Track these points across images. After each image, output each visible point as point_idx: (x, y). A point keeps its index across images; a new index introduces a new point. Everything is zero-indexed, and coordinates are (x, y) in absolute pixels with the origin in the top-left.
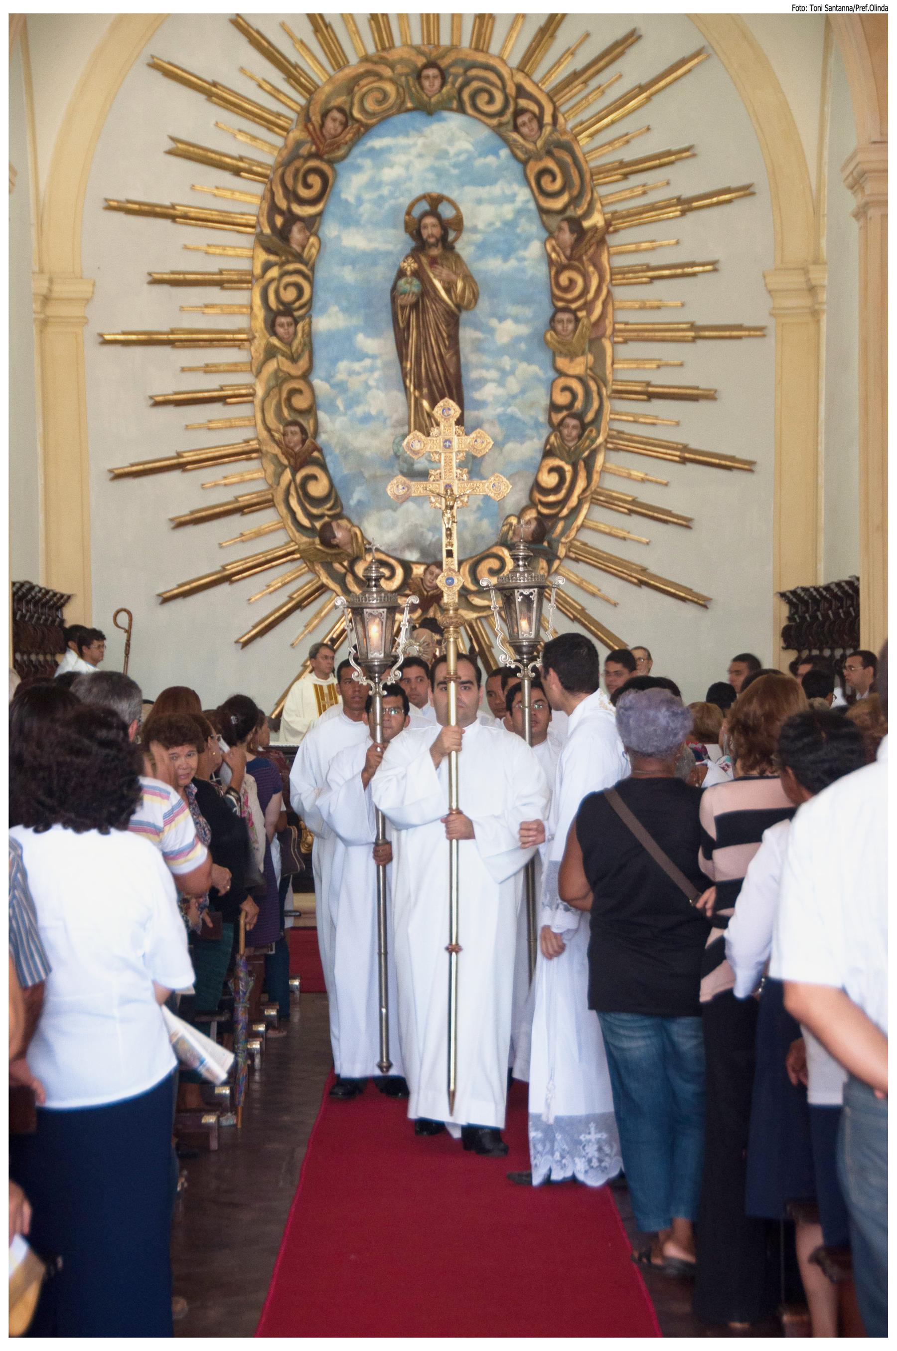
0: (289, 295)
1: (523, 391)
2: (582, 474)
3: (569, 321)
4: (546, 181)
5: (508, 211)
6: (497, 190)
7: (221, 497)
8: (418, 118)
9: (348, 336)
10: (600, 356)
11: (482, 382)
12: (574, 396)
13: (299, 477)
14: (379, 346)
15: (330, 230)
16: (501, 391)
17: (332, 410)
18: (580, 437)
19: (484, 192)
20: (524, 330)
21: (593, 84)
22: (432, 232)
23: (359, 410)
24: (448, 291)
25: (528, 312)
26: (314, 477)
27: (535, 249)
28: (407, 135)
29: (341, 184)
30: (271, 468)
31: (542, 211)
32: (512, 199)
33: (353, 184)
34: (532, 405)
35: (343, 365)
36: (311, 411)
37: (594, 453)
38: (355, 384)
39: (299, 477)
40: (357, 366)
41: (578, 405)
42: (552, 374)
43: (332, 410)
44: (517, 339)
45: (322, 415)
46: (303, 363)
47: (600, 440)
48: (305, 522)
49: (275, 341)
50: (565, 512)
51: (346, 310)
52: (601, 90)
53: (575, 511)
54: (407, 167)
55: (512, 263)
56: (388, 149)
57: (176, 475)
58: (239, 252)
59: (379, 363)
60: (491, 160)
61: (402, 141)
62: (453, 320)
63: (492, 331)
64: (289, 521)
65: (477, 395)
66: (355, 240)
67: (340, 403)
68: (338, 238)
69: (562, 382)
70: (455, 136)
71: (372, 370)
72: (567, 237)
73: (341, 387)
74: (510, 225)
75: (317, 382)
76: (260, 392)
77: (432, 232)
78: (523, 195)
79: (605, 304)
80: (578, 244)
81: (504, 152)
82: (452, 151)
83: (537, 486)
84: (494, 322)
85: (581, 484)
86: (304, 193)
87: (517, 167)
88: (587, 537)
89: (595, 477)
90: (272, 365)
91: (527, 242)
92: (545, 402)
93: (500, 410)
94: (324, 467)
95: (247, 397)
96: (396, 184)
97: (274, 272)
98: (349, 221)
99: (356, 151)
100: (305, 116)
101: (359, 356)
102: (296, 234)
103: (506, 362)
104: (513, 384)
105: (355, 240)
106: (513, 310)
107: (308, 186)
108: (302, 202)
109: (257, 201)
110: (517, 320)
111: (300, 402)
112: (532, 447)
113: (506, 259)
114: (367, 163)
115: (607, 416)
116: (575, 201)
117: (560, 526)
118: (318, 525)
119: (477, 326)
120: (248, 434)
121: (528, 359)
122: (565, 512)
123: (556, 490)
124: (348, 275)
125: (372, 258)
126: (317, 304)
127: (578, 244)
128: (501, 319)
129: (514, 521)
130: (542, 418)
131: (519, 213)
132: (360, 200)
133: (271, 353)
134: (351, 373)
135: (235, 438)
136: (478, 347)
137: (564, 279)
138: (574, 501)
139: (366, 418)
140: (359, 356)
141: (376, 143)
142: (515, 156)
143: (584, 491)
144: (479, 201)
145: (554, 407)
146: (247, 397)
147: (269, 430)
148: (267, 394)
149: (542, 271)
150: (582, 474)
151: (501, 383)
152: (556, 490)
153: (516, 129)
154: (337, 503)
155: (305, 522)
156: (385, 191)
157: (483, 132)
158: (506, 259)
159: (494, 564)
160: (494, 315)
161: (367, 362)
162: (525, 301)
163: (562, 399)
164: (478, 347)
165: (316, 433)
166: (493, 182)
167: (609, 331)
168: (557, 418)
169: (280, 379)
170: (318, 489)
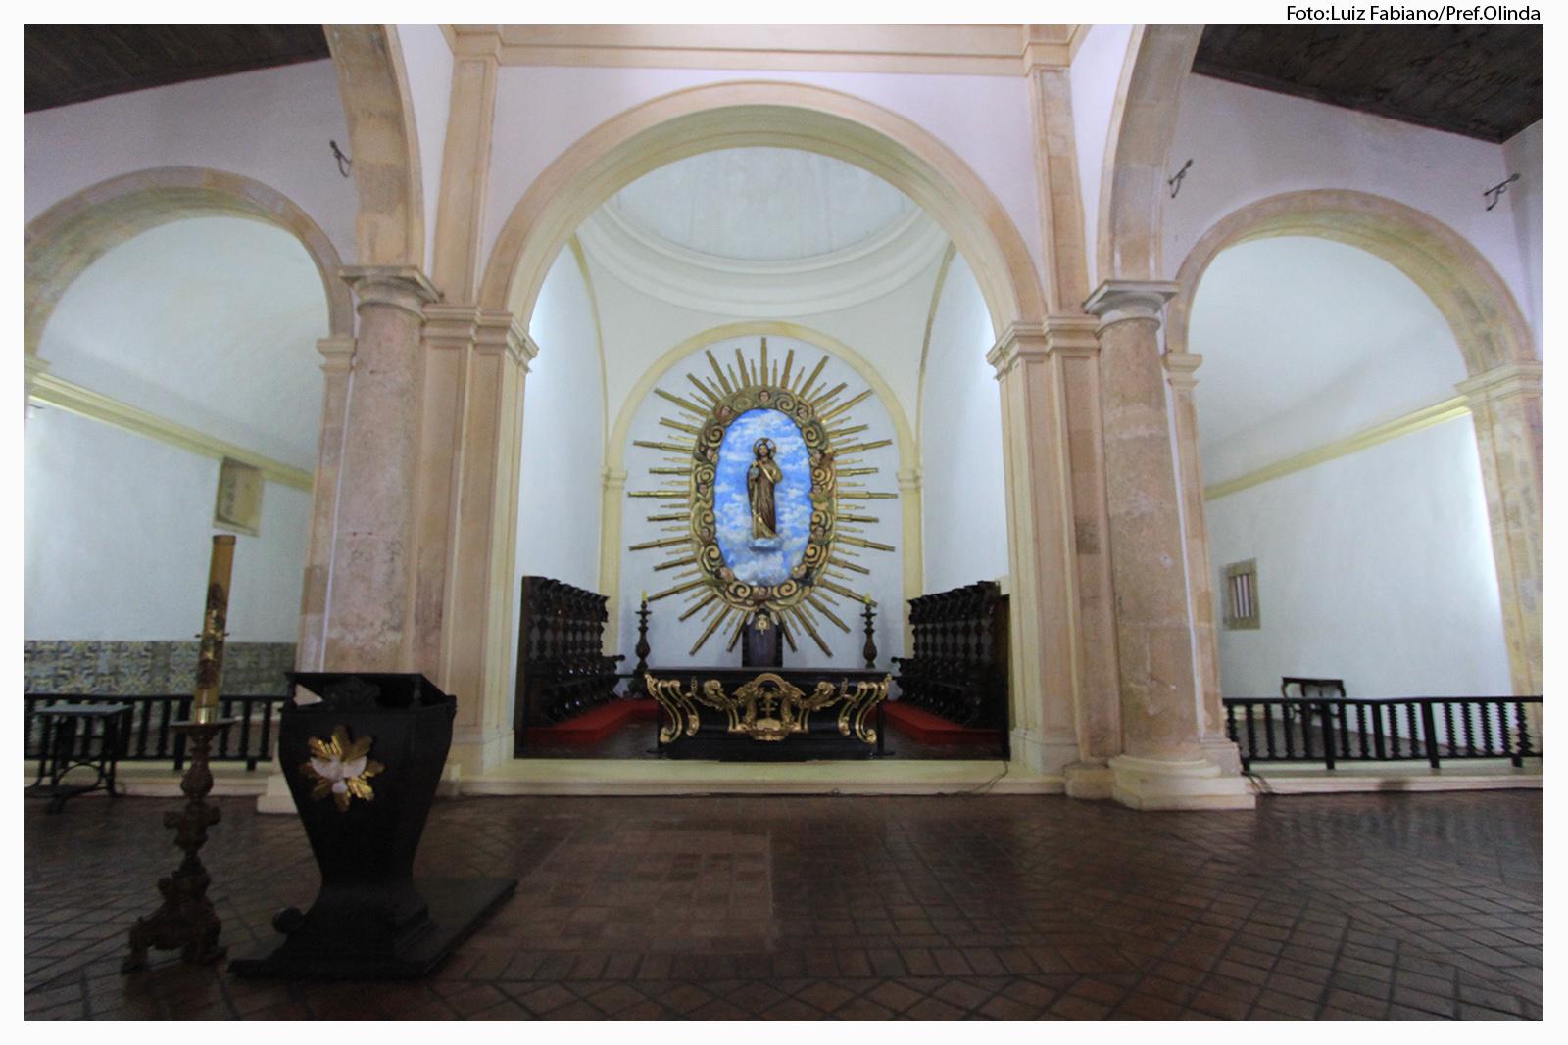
0: (705, 477)
1: (800, 517)
4: (810, 436)
5: (794, 447)
6: (790, 439)
7: (676, 558)
8: (759, 412)
9: (729, 494)
10: (831, 504)
11: (783, 513)
12: (821, 518)
13: (707, 550)
14: (741, 498)
15: (723, 453)
16: (791, 517)
17: (722, 523)
19: (785, 439)
20: (801, 493)
21: (829, 401)
22: (764, 453)
23: (733, 524)
24: (771, 474)
25: (801, 486)
26: (712, 550)
27: (805, 462)
28: (754, 417)
29: (728, 437)
30: (695, 546)
31: (807, 446)
32: (795, 442)
33: (733, 436)
34: (804, 522)
35: (727, 506)
36: (713, 523)
37: (829, 542)
38: (731, 513)
39: (707, 550)
40: (732, 506)
41: (823, 523)
42: (811, 510)
43: (722, 523)
44: (798, 497)
45: (718, 526)
46: (710, 504)
47: (832, 537)
48: (709, 568)
49: (699, 495)
50: (817, 566)
51: (729, 484)
52: (831, 403)
53: (821, 566)
54: (755, 429)
55: (796, 467)
56: (746, 423)
57: (656, 549)
58: (686, 461)
59: (741, 505)
60: (788, 428)
61: (753, 420)
62: (772, 486)
63: (787, 493)
64: (702, 568)
65: (782, 518)
66: (732, 457)
67: (725, 521)
68: (726, 457)
69: (816, 513)
70: (774, 419)
71: (738, 507)
72: (818, 456)
73: (726, 514)
74: (795, 452)
75: (716, 512)
76: (692, 515)
77: (764, 453)
78: (800, 441)
79: (833, 483)
80: (823, 460)
81: (793, 425)
82: (773, 423)
83: (806, 555)
84: (788, 490)
85: (824, 554)
86: (713, 438)
87: (798, 430)
88: (826, 577)
89: (830, 553)
90: (698, 505)
91: (801, 459)
92: (808, 521)
93: (790, 525)
94: (717, 546)
95: (687, 517)
96: (750, 435)
97: (700, 469)
98: (730, 449)
99: (735, 423)
100: (715, 410)
101: (733, 502)
102: (709, 453)
103: (793, 505)
104: (796, 514)
105: (732, 457)
106: (795, 484)
107: (714, 435)
108: (712, 441)
109: (694, 442)
110: (797, 488)
111: (709, 519)
112: (804, 539)
113: (794, 464)
114: (739, 428)
115: (834, 527)
116: (821, 443)
117: (815, 572)
118: (714, 570)
119: (782, 491)
120: (687, 532)
121: (803, 504)
122: (817, 566)
123: (814, 556)
124: (730, 470)
125: (739, 464)
126: (717, 481)
127: (823, 460)
128: (792, 488)
129: (796, 569)
130: (808, 528)
131: (799, 448)
132: (735, 442)
133: (697, 500)
134: (730, 509)
135: (682, 534)
136: (782, 499)
137: (817, 473)
138: (821, 561)
139: (736, 527)
140: (733, 502)
141: (742, 420)
142: (797, 426)
144: (783, 443)
145: (813, 523)
146: (687, 517)
147: (695, 530)
148: (695, 516)
149: (807, 470)
151: (791, 513)
152: (814, 556)
153: (798, 415)
154: (723, 560)
155: (709, 568)
156: (746, 439)
157: (785, 418)
158: (794, 464)
159: (787, 587)
160: (788, 486)
161: (736, 505)
162: (802, 481)
163: (816, 520)
164: (782, 499)
165: (715, 532)
166: (788, 435)
168: (814, 527)
169: (701, 510)
170: (715, 555)
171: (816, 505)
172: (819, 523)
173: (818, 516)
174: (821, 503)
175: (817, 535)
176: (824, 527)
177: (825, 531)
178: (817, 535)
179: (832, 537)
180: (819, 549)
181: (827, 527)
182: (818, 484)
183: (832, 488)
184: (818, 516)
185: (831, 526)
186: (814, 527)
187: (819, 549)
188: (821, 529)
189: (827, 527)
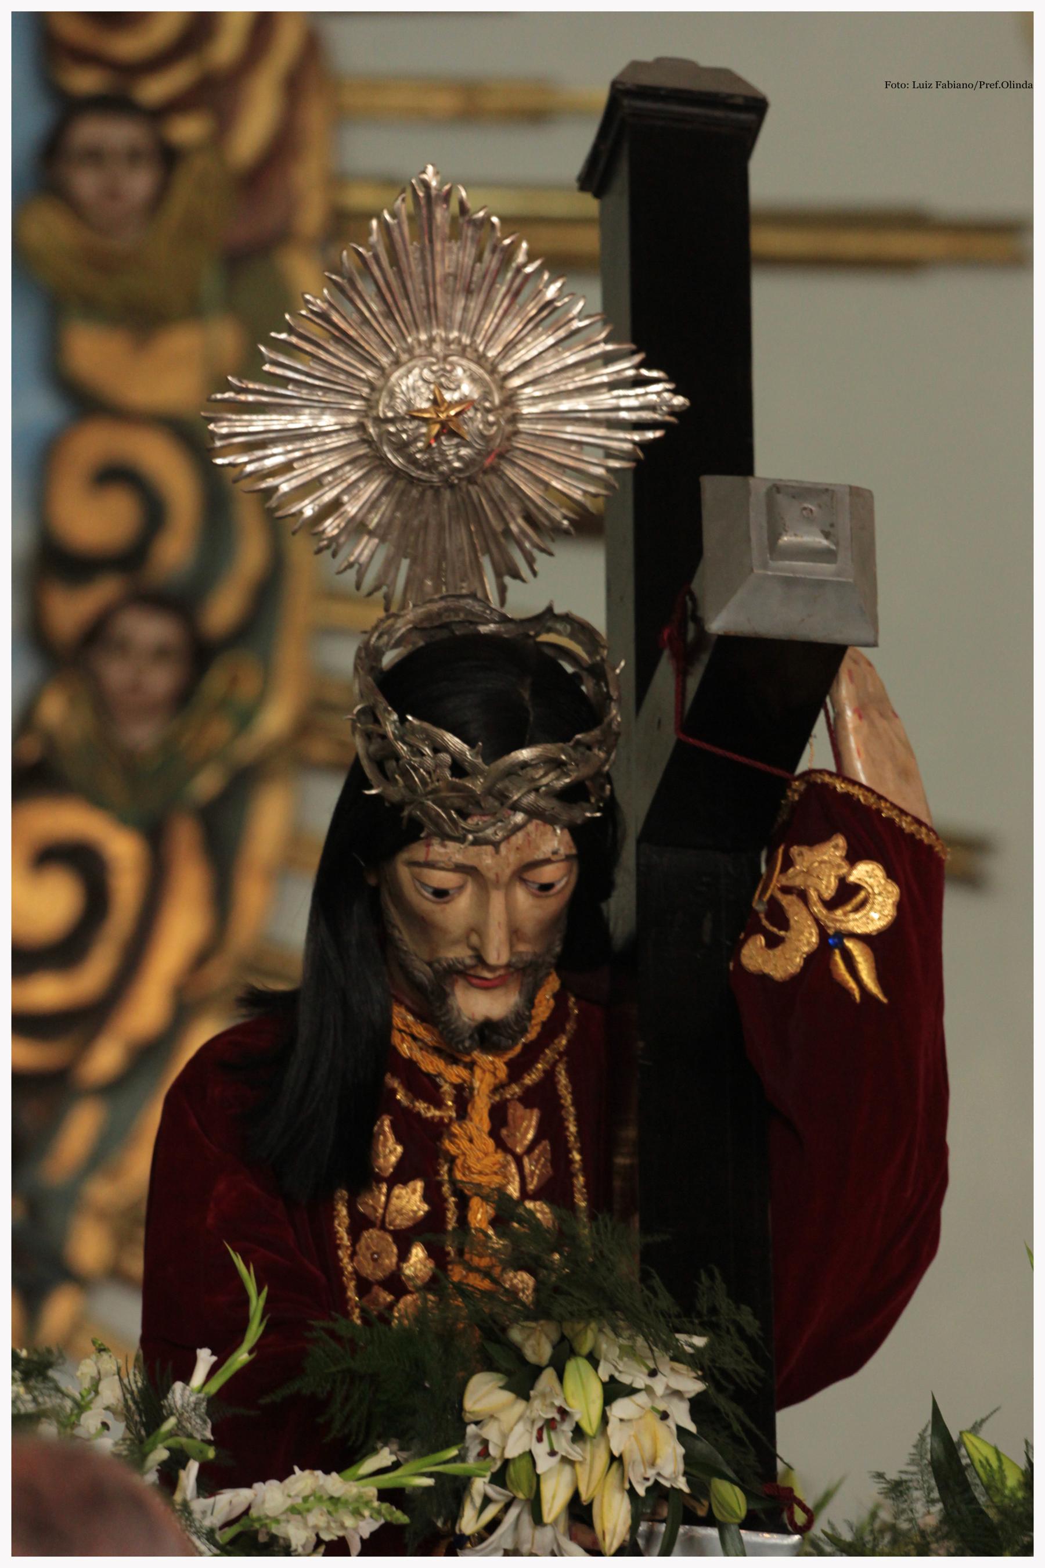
2: (189, 884)
3: (133, 156)
12: (154, 513)
18: (184, 699)
37: (244, 782)
41: (175, 551)
47: (275, 719)
50: (106, 1058)
69: (96, 443)
85: (182, 929)
122: (106, 1058)
143: (202, 958)
150: (189, 884)
163: (96, 521)
167: (311, 217)
168: (71, 610)
171: (93, 351)
172: (131, 559)
173: (116, 475)
174: (144, 321)
175: (102, 706)
176: (181, 602)
177: (200, 654)
178: (102, 706)
179: (275, 719)
180: (123, 850)
181: (224, 609)
182: (115, 103)
183: (283, 147)
184: (116, 475)
185: (268, 593)
186: (71, 610)
187: (123, 850)
188: (149, 629)
189: (224, 609)
